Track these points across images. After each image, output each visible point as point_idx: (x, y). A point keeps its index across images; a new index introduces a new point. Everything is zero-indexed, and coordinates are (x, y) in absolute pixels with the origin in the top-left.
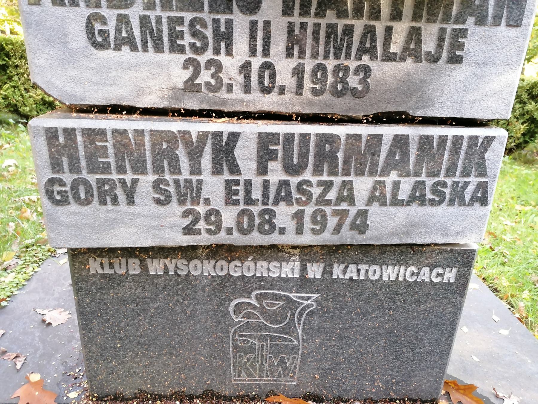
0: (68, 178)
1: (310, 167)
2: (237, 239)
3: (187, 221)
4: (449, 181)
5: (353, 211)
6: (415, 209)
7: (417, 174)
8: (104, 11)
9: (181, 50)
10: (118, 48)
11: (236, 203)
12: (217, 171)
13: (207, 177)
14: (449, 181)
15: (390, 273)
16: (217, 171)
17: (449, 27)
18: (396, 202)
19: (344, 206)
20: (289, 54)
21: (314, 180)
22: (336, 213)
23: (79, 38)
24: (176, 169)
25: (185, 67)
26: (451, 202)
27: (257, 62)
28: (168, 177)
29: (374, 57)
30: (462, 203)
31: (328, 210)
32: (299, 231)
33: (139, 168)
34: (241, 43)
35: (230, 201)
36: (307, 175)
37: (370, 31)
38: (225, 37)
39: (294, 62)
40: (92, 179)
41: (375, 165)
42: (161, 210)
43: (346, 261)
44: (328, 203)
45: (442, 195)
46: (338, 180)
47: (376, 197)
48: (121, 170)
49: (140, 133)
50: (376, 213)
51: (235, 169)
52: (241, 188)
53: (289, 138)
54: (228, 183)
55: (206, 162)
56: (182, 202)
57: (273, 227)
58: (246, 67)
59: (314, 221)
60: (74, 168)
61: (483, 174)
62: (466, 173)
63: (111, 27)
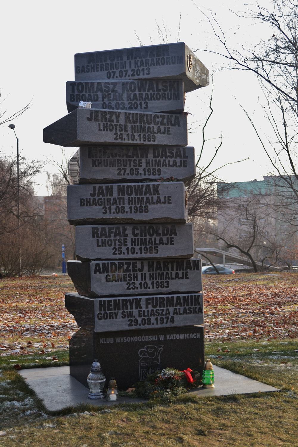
0: (103, 312)
1: (158, 306)
2: (142, 327)
3: (129, 323)
4: (192, 307)
5: (170, 317)
6: (185, 315)
7: (184, 306)
8: (110, 274)
9: (126, 281)
10: (112, 281)
11: (141, 316)
12: (136, 308)
13: (134, 310)
14: (192, 307)
15: (182, 336)
16: (136, 308)
17: (184, 271)
18: (180, 314)
19: (167, 316)
20: (150, 280)
21: (159, 309)
22: (166, 318)
23: (104, 280)
24: (127, 309)
25: (127, 284)
26: (194, 313)
27: (143, 282)
28: (125, 310)
29: (169, 279)
30: (196, 313)
31: (164, 317)
32: (157, 324)
33: (119, 309)
34: (139, 277)
35: (140, 316)
36: (158, 308)
37: (167, 273)
38: (136, 277)
39: (152, 281)
40: (108, 312)
41: (173, 304)
42: (124, 320)
43: (170, 334)
44: (164, 315)
45: (191, 311)
46: (165, 308)
47: (175, 312)
48: (115, 310)
49: (119, 300)
50: (176, 317)
51: (141, 308)
52: (142, 312)
53: (153, 298)
54: (139, 311)
55: (134, 306)
56: (128, 317)
57: (150, 322)
58: (141, 284)
59: (161, 321)
60: (105, 310)
61: (199, 304)
62: (195, 305)
63: (111, 277)
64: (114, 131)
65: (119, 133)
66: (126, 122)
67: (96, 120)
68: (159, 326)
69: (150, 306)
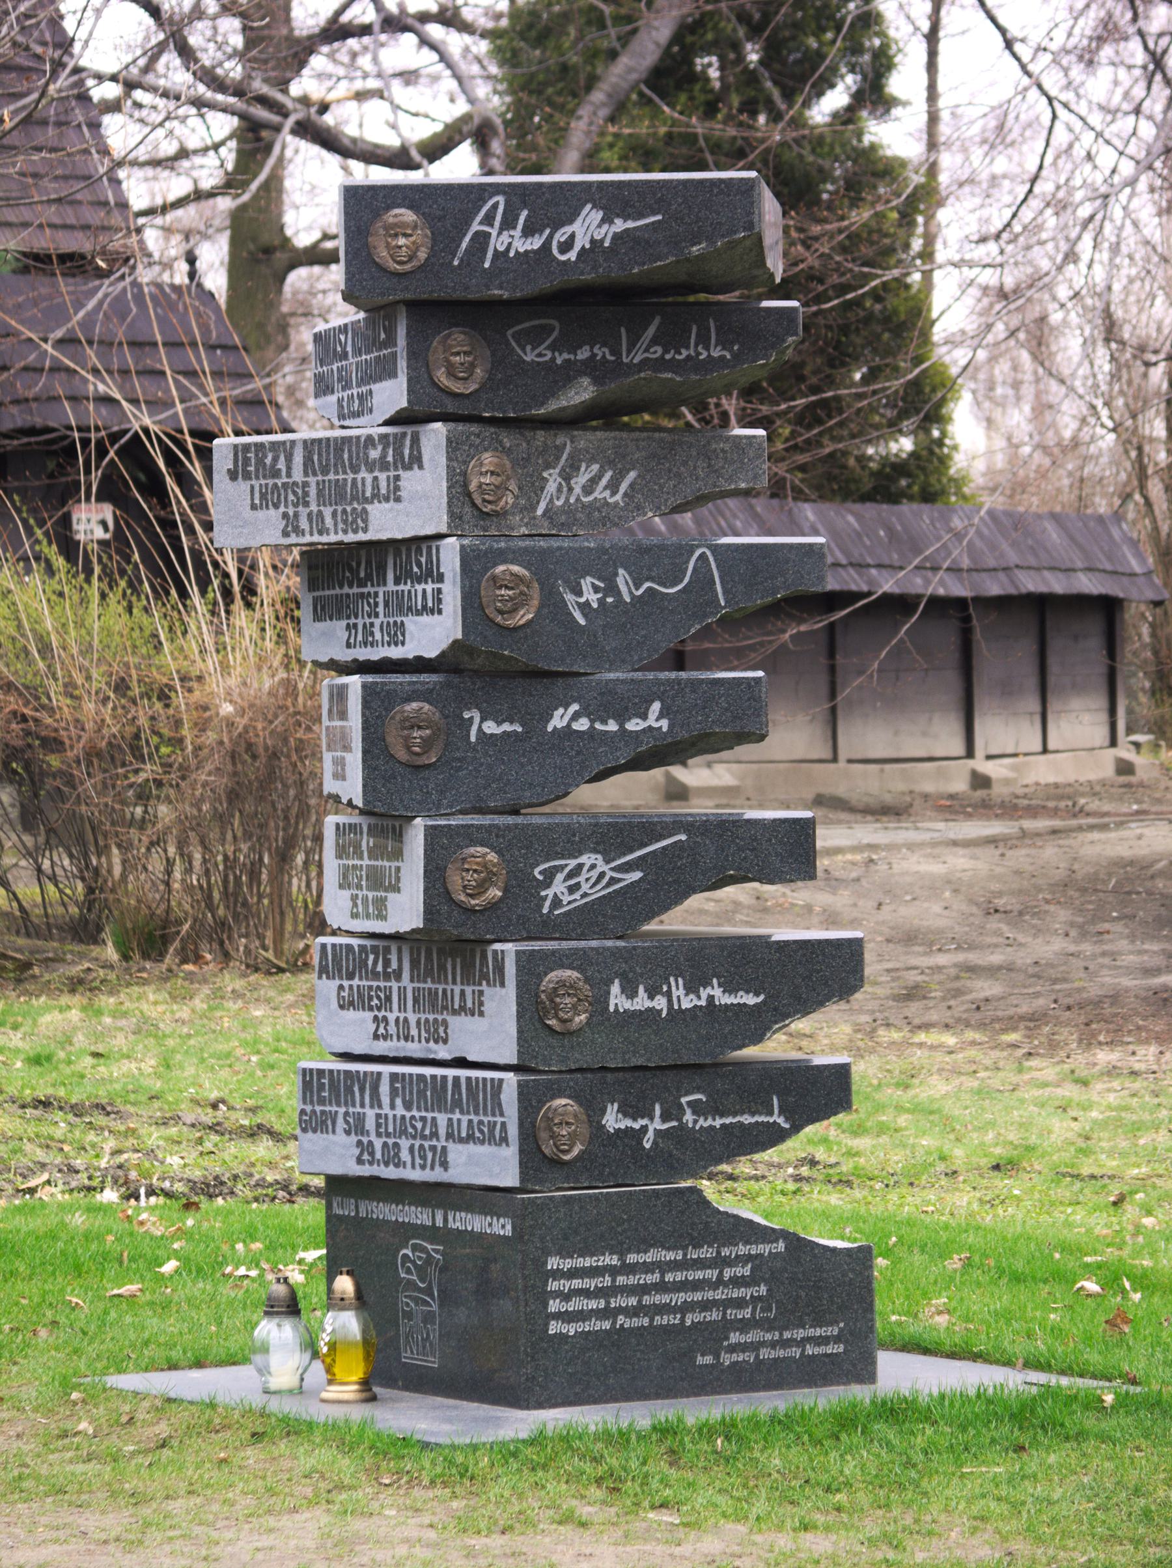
35: (379, 1135)
40: (318, 1108)
46: (429, 1115)
50: (458, 1153)
54: (378, 1116)
64: (282, 509)
65: (291, 512)
66: (306, 474)
67: (247, 476)
68: (415, 1175)
69: (399, 1101)
